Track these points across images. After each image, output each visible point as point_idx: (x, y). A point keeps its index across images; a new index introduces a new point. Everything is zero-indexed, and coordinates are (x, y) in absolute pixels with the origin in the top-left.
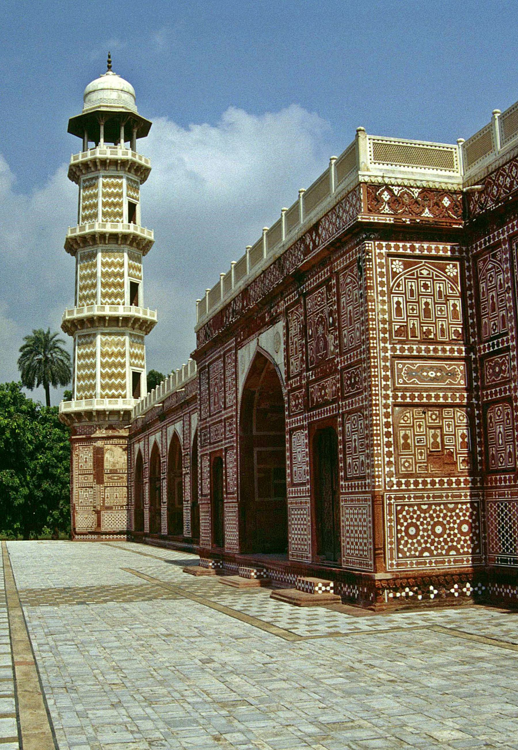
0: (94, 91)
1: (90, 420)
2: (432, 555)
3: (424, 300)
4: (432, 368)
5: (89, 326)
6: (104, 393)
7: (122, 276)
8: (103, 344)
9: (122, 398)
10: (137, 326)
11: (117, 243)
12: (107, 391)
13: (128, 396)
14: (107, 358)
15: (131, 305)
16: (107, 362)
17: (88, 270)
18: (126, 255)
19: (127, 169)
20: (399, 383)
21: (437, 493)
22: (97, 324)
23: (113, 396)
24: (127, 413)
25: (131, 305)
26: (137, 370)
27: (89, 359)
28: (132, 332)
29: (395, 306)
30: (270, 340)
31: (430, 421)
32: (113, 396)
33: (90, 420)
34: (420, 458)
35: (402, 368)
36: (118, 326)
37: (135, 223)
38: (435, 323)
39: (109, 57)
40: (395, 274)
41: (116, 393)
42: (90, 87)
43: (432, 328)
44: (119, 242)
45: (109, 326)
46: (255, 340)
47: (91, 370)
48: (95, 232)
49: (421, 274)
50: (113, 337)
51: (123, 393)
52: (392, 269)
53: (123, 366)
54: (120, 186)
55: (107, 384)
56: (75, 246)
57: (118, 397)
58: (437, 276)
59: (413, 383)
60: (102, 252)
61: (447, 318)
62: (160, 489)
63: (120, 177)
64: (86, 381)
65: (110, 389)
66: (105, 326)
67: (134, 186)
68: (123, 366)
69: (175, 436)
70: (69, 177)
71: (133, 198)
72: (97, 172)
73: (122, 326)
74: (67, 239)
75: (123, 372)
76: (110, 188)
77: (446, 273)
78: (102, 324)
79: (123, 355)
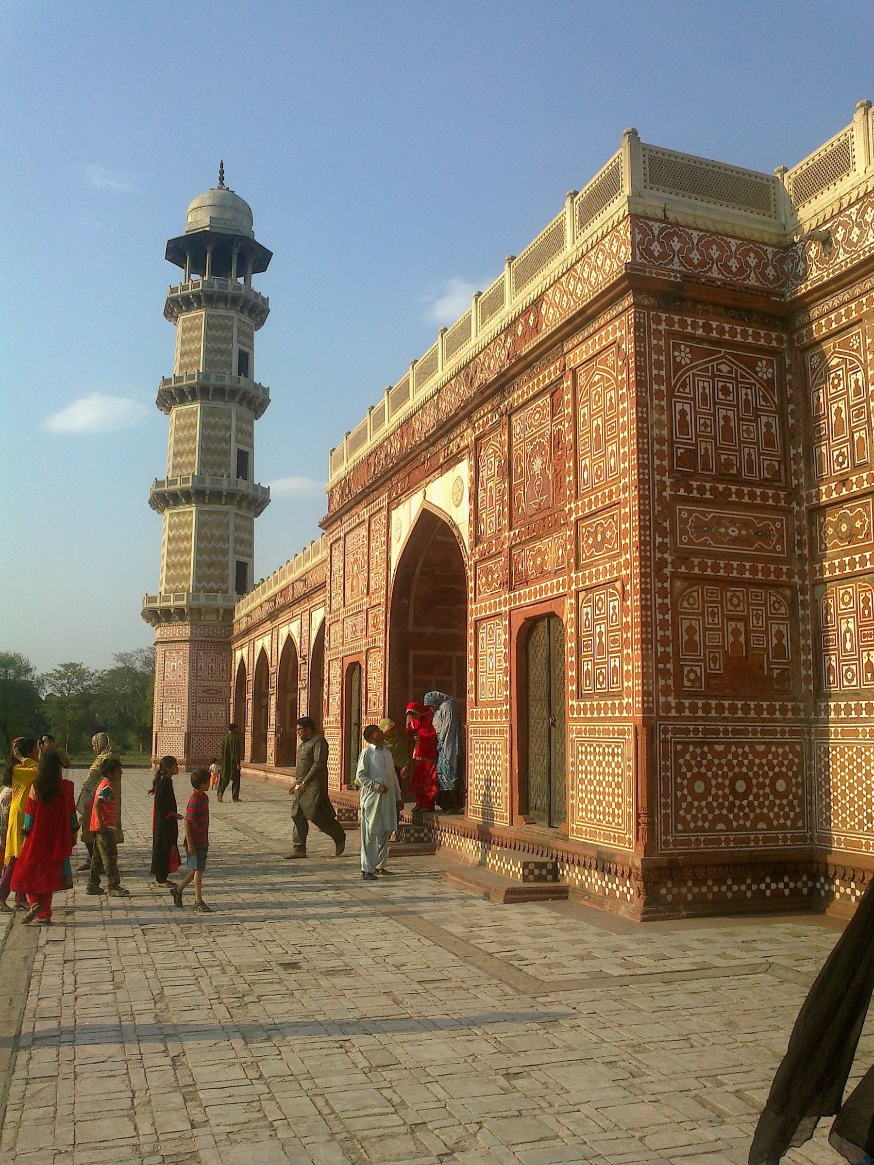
2: (730, 828)
3: (722, 413)
4: (733, 521)
6: (200, 586)
7: (228, 441)
9: (223, 593)
10: (244, 504)
11: (223, 400)
13: (230, 590)
15: (238, 477)
19: (239, 308)
20: (682, 542)
21: (739, 725)
22: (193, 499)
23: (211, 590)
29: (678, 417)
30: (447, 492)
31: (730, 607)
32: (211, 590)
34: (712, 666)
35: (688, 519)
36: (220, 503)
37: (246, 376)
38: (739, 451)
40: (678, 366)
43: (734, 458)
44: (226, 398)
45: (210, 503)
46: (421, 493)
49: (719, 370)
52: (675, 357)
58: (743, 377)
59: (703, 544)
61: (757, 443)
62: (267, 707)
65: (208, 582)
68: (225, 553)
69: (289, 638)
71: (245, 345)
73: (226, 504)
76: (217, 330)
77: (757, 373)
79: (226, 540)
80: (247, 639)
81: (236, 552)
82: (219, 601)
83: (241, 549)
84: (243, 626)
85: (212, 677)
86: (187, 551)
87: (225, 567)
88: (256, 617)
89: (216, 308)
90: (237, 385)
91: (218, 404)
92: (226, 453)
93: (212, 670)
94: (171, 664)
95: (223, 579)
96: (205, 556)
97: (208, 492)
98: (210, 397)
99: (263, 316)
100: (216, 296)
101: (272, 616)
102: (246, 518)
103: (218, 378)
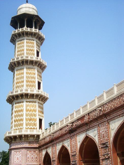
0: (22, 8)
5: (20, 98)
6: (27, 127)
8: (27, 106)
11: (32, 65)
12: (28, 126)
14: (28, 112)
16: (29, 114)
17: (20, 76)
18: (36, 70)
19: (36, 37)
23: (31, 128)
24: (38, 136)
26: (41, 118)
27: (20, 112)
28: (39, 102)
32: (31, 128)
33: (21, 140)
36: (33, 98)
41: (32, 127)
42: (20, 7)
44: (34, 64)
45: (30, 98)
47: (21, 117)
48: (24, 59)
50: (31, 103)
51: (35, 127)
53: (35, 115)
54: (33, 43)
55: (29, 123)
56: (14, 66)
60: (26, 68)
63: (34, 40)
64: (19, 122)
65: (30, 126)
66: (27, 98)
67: (38, 46)
68: (35, 115)
70: (11, 41)
72: (24, 37)
73: (35, 99)
74: (11, 63)
75: (35, 118)
78: (26, 97)
81: (39, 115)
82: (35, 132)
84: (48, 139)
85: (32, 161)
87: (35, 120)
89: (28, 37)
92: (34, 82)
93: (32, 158)
96: (28, 117)
97: (29, 94)
98: (28, 64)
99: (43, 41)
102: (41, 104)
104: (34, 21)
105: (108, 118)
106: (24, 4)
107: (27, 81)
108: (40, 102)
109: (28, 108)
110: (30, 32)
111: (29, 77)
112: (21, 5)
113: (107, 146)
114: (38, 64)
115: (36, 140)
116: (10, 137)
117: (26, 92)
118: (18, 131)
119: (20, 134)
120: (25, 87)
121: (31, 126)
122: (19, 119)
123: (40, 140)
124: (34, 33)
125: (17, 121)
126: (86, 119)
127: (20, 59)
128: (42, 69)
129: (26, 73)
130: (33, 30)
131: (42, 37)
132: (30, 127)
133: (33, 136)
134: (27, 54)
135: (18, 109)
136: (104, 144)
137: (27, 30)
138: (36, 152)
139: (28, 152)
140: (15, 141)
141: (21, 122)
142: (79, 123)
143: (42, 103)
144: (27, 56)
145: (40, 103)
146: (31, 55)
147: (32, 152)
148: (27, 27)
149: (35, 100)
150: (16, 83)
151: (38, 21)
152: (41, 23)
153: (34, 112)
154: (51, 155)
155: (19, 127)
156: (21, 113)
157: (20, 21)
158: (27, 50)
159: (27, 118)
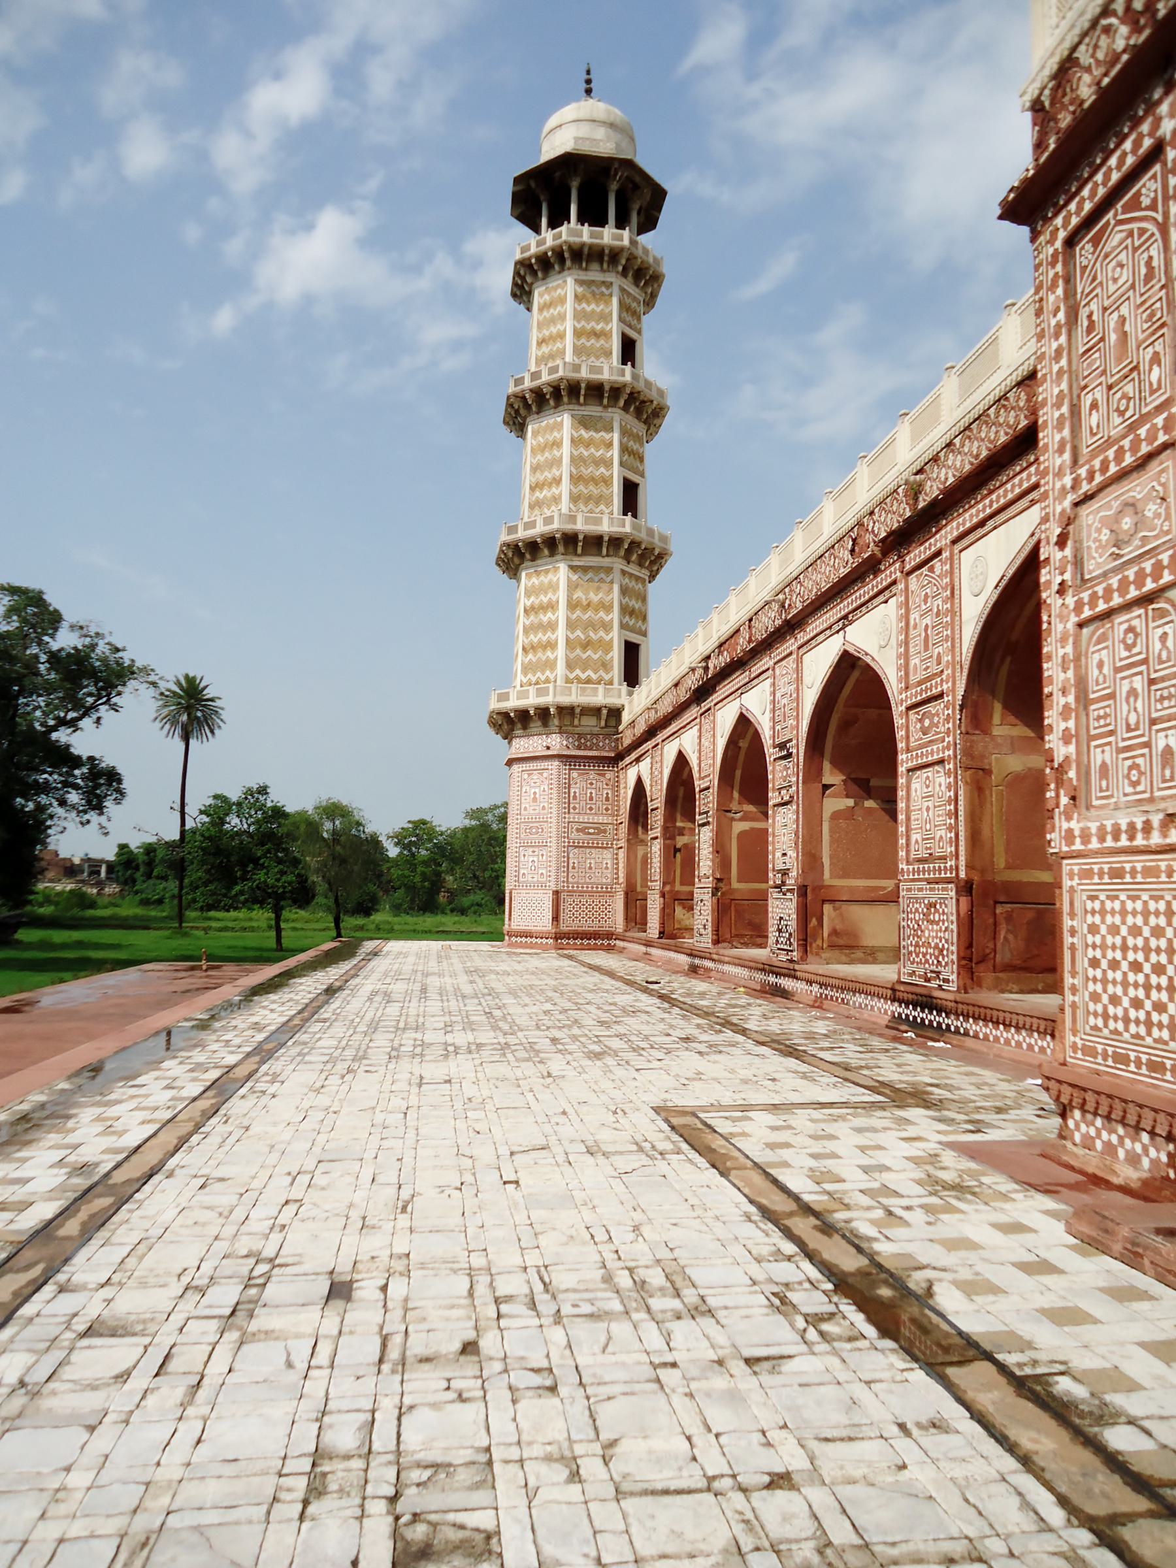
1: (545, 724)
5: (546, 552)
6: (572, 676)
7: (608, 464)
10: (634, 557)
11: (601, 404)
12: (578, 672)
13: (616, 681)
14: (578, 613)
16: (578, 619)
17: (547, 454)
19: (620, 268)
22: (561, 548)
23: (588, 681)
24: (615, 713)
25: (625, 514)
27: (545, 613)
32: (588, 681)
33: (545, 724)
36: (599, 554)
39: (588, 72)
41: (594, 677)
42: (553, 121)
44: (605, 401)
45: (584, 554)
53: (607, 627)
55: (578, 657)
56: (523, 412)
57: (599, 683)
64: (540, 654)
66: (576, 554)
70: (514, 295)
71: (630, 326)
74: (508, 398)
75: (608, 638)
80: (649, 745)
82: (599, 697)
83: (631, 623)
84: (641, 728)
86: (552, 626)
87: (608, 647)
88: (666, 707)
90: (621, 379)
91: (594, 410)
92: (607, 482)
94: (529, 790)
95: (606, 666)
96: (578, 633)
100: (586, 250)
101: (702, 693)
102: (638, 578)
103: (592, 369)
104: (614, 186)
105: (802, 637)
106: (573, 106)
107: (575, 479)
108: (633, 569)
109: (578, 594)
110: (591, 246)
111: (584, 462)
112: (558, 114)
113: (789, 755)
114: (626, 396)
115: (606, 726)
116: (505, 715)
117: (569, 527)
118: (532, 690)
119: (542, 701)
120: (565, 505)
121: (589, 673)
122: (540, 642)
123: (621, 728)
124: (612, 249)
125: (533, 647)
126: (742, 644)
127: (545, 378)
128: (645, 422)
129: (573, 441)
130: (609, 236)
131: (647, 269)
132: (583, 676)
133: (596, 711)
134: (577, 351)
135: (537, 602)
136: (782, 746)
137: (577, 240)
138: (608, 776)
139: (575, 774)
140: (525, 728)
141: (549, 653)
142: (725, 659)
143: (644, 574)
144: (577, 361)
145: (631, 575)
146: (597, 358)
147: (592, 775)
148: (581, 220)
149: (608, 560)
150: (532, 489)
151: (636, 187)
152: (647, 194)
153: (602, 614)
154: (648, 789)
155: (539, 674)
156: (549, 614)
157: (545, 191)
158: (578, 334)
159: (572, 637)
